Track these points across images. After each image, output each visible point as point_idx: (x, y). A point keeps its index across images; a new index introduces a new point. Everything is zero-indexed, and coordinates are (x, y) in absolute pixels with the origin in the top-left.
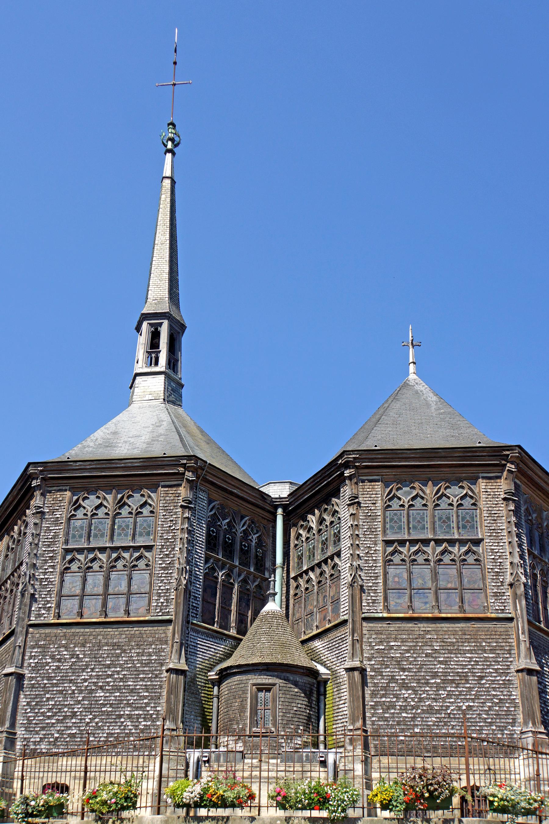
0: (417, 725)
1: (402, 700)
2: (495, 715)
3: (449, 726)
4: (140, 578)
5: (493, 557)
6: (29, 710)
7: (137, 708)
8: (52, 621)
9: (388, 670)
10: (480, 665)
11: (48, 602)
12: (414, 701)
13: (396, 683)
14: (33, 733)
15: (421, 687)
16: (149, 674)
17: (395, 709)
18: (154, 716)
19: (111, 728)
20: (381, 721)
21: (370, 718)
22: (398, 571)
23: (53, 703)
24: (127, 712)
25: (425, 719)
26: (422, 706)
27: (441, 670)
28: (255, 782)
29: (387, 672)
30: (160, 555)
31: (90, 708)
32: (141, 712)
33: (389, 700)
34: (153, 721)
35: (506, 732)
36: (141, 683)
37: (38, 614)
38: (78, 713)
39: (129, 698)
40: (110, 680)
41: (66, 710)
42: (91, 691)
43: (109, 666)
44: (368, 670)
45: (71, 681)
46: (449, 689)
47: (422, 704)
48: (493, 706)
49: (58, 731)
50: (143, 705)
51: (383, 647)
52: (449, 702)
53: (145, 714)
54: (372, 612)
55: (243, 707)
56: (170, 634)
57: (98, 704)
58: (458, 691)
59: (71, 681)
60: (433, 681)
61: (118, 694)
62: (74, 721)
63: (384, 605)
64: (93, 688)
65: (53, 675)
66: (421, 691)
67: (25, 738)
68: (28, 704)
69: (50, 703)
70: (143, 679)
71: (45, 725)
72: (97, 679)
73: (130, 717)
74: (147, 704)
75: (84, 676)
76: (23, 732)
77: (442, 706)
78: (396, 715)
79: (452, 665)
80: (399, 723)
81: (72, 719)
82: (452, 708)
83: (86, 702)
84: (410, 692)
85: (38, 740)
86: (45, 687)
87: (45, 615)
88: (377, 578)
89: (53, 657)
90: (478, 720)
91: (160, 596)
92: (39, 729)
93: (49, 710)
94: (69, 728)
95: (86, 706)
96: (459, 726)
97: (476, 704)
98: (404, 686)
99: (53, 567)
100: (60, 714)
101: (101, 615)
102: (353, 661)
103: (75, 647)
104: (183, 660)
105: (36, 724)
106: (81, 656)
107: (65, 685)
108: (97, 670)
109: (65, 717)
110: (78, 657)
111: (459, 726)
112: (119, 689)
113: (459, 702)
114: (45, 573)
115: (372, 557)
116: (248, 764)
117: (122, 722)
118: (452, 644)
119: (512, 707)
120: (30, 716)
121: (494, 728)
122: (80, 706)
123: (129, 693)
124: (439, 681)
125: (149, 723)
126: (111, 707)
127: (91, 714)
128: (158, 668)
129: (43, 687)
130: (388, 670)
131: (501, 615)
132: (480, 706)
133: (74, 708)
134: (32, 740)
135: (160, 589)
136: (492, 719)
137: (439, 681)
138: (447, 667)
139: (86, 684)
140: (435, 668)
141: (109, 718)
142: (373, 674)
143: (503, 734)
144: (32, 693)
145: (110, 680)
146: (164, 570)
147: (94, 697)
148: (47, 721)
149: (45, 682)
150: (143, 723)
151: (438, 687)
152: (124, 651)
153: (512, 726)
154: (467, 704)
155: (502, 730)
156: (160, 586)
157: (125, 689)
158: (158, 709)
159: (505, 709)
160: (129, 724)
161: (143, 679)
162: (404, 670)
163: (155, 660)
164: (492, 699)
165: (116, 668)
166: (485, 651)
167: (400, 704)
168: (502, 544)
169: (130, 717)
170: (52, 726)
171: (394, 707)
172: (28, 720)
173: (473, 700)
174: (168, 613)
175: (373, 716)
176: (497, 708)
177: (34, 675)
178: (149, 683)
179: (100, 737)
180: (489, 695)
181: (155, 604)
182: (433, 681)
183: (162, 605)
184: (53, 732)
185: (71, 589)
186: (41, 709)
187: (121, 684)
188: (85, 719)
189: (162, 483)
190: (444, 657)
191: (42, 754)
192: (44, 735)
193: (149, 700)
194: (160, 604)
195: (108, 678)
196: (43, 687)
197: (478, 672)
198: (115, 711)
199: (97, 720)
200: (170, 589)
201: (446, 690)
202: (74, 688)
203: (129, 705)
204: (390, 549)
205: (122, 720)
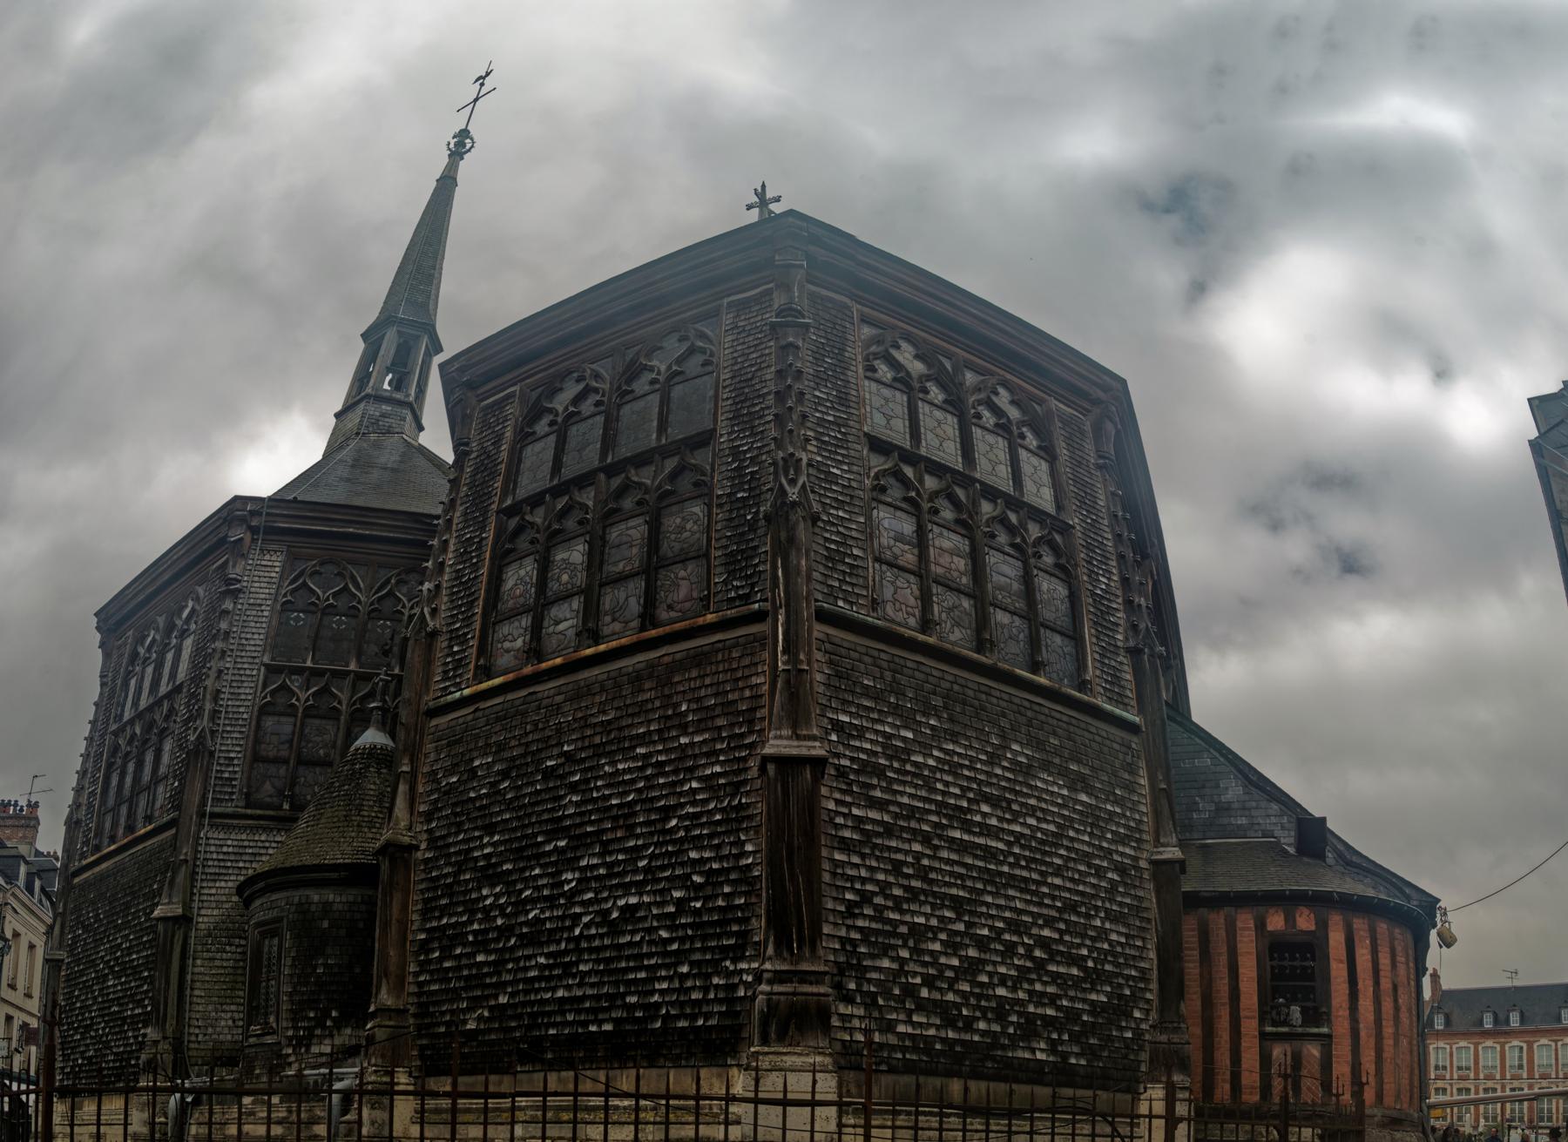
2: (690, 925)
46: (584, 863)
52: (583, 903)
58: (605, 864)
79: (598, 789)
82: (586, 919)
111: (597, 972)
113: (606, 900)
119: (740, 894)
121: (685, 969)
124: (562, 843)
137: (562, 843)
138: (588, 796)
143: (706, 989)
151: (567, 860)
153: (735, 961)
154: (621, 903)
155: (708, 976)
159: (720, 903)
164: (688, 876)
166: (684, 729)
173: (639, 887)
176: (698, 905)
180: (682, 864)
190: (581, 771)
197: (659, 798)
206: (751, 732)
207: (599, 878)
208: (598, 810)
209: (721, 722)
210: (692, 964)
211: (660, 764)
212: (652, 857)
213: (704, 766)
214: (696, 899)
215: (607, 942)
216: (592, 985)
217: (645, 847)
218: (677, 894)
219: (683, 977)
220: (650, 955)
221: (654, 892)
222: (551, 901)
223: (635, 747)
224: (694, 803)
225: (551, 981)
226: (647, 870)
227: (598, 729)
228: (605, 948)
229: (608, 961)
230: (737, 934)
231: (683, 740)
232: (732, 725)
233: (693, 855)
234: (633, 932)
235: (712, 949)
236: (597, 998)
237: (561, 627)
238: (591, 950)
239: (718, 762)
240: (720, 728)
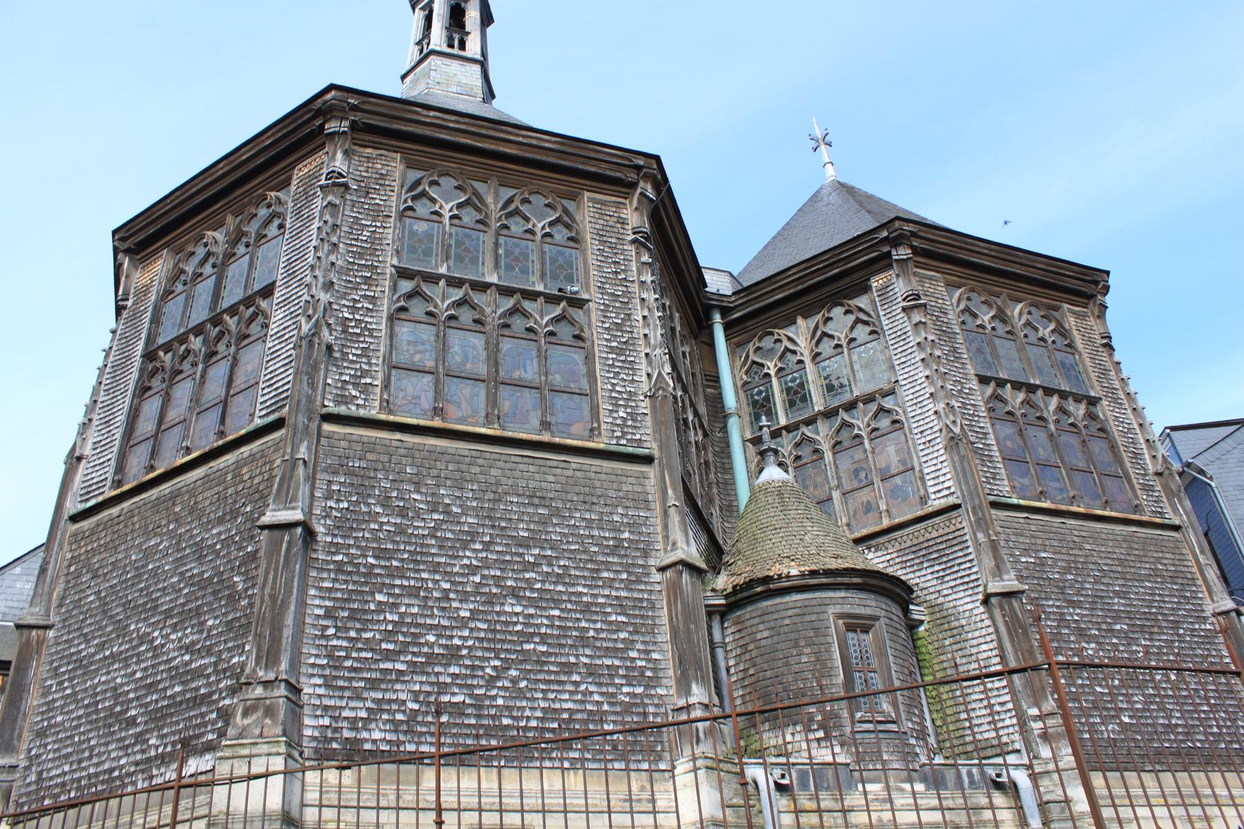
6: (331, 631)
11: (365, 373)
14: (347, 694)
18: (649, 674)
19: (552, 696)
23: (396, 618)
31: (493, 640)
32: (617, 663)
34: (647, 687)
36: (607, 592)
38: (464, 652)
41: (432, 638)
42: (490, 600)
43: (524, 543)
45: (435, 568)
50: (621, 646)
53: (627, 668)
55: (824, 666)
59: (435, 568)
61: (557, 613)
62: (454, 669)
64: (494, 590)
67: (326, 708)
68: (329, 614)
69: (389, 617)
70: (609, 583)
71: (378, 675)
73: (592, 671)
75: (470, 557)
76: (321, 691)
81: (449, 665)
85: (364, 714)
86: (369, 574)
87: (360, 402)
89: (385, 502)
92: (362, 684)
93: (389, 635)
95: (482, 635)
99: (372, 299)
100: (416, 650)
106: (455, 509)
112: (557, 602)
117: (576, 684)
122: (466, 633)
123: (581, 612)
125: (639, 690)
126: (543, 643)
128: (640, 562)
129: (365, 575)
133: (452, 637)
134: (346, 713)
139: (477, 579)
141: (541, 671)
144: (337, 586)
145: (533, 575)
147: (498, 613)
148: (382, 666)
149: (371, 560)
150: (625, 689)
152: (557, 512)
156: (613, 385)
157: (570, 601)
158: (655, 656)
160: (592, 688)
161: (609, 583)
163: (630, 541)
169: (592, 671)
170: (397, 681)
172: (330, 656)
178: (623, 594)
179: (528, 718)
184: (403, 696)
185: (412, 356)
186: (365, 630)
187: (560, 588)
188: (482, 668)
191: (376, 757)
195: (527, 571)
196: (365, 575)
199: (513, 673)
202: (447, 586)
203: (583, 641)
205: (576, 678)
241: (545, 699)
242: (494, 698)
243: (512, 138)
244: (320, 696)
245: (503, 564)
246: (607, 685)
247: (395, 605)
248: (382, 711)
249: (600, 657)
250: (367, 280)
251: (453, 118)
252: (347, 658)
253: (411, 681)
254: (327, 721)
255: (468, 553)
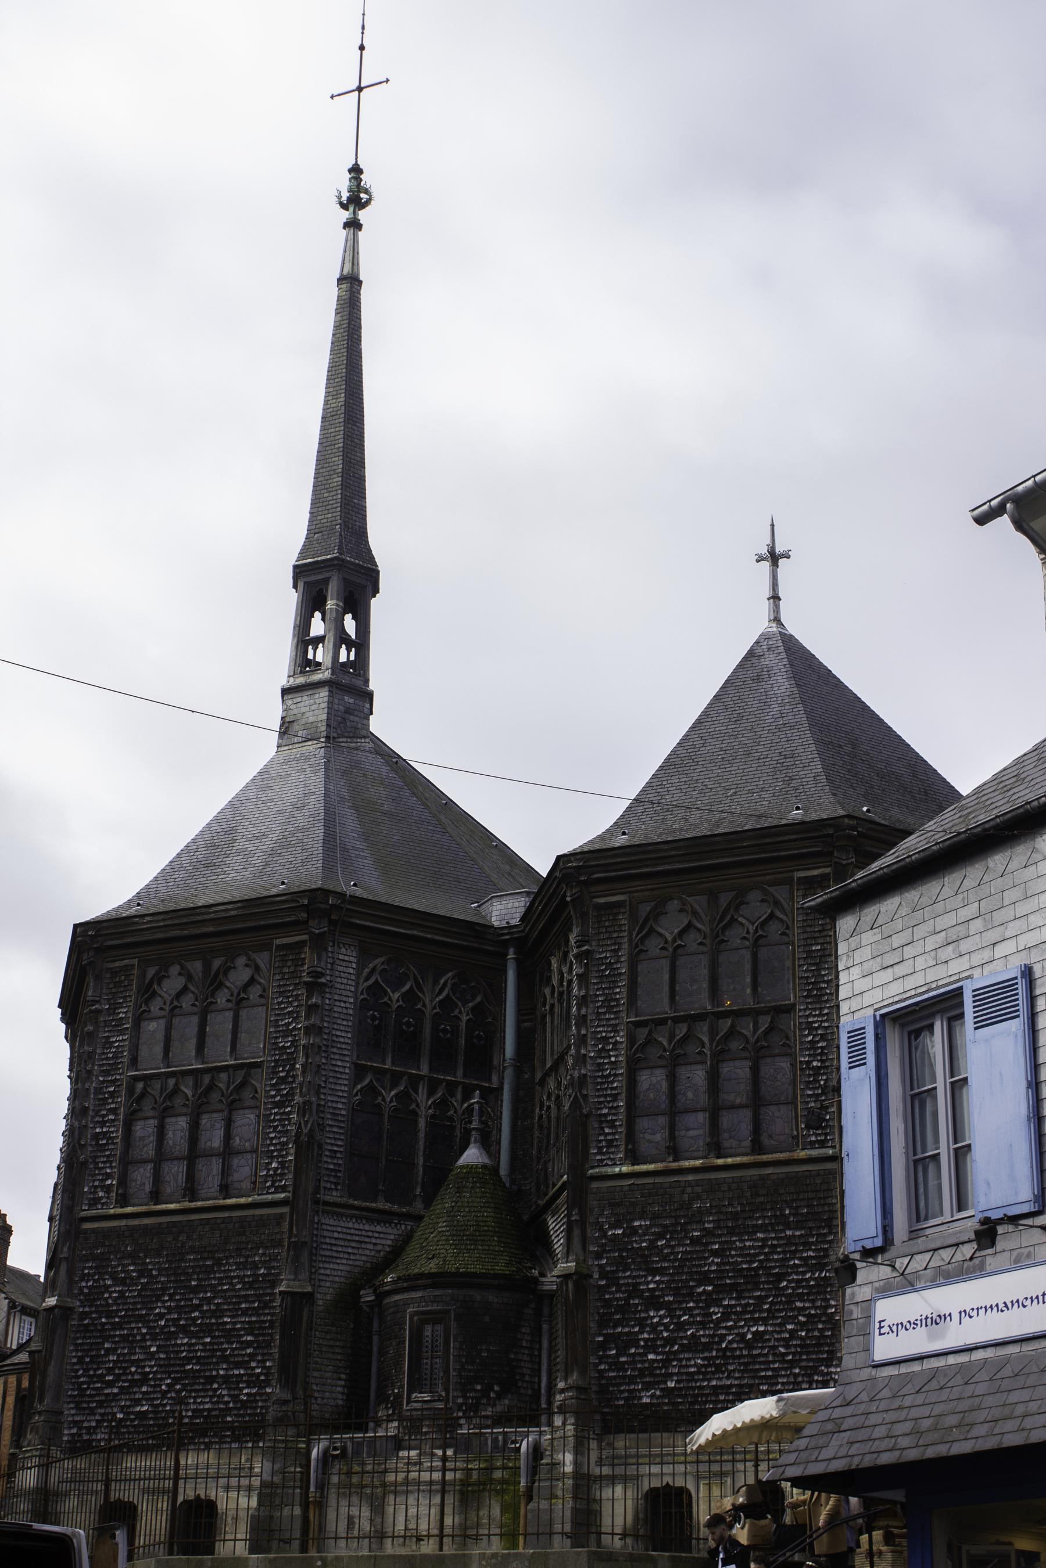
0: (672, 1374)
1: (648, 1329)
2: (800, 1346)
3: (723, 1373)
4: (246, 1121)
5: (810, 1038)
6: (81, 1372)
7: (238, 1365)
8: (112, 1211)
9: (628, 1273)
10: (779, 1253)
11: (109, 1176)
12: (667, 1329)
13: (641, 1297)
14: (87, 1412)
15: (680, 1303)
16: (254, 1302)
17: (637, 1347)
18: (262, 1378)
19: (199, 1400)
20: (613, 1371)
21: (596, 1365)
22: (654, 1080)
24: (221, 1372)
25: (684, 1363)
26: (682, 1338)
27: (714, 1268)
28: (412, 1492)
29: (625, 1276)
30: (272, 1079)
32: (242, 1372)
33: (626, 1330)
34: (260, 1388)
35: (816, 1378)
37: (94, 1199)
39: (225, 1346)
40: (197, 1314)
41: (133, 1369)
44: (596, 1276)
47: (681, 1334)
48: (797, 1331)
49: (122, 1407)
50: (246, 1359)
51: (620, 1232)
52: (726, 1328)
54: (607, 1165)
56: (286, 1224)
57: (180, 1359)
59: (140, 1318)
60: (701, 1289)
61: (208, 1340)
62: (144, 1389)
63: (626, 1151)
64: (172, 1329)
65: (115, 1308)
66: (681, 1309)
67: (75, 1422)
69: (111, 1358)
70: (245, 1312)
71: (103, 1398)
72: (179, 1313)
73: (226, 1380)
74: (252, 1357)
76: (73, 1412)
77: (713, 1336)
78: (638, 1358)
79: (733, 1256)
80: (642, 1373)
81: (141, 1386)
83: (162, 1356)
84: (662, 1312)
85: (94, 1424)
88: (615, 1098)
89: (114, 1276)
90: (771, 1358)
91: (272, 1158)
93: (110, 1371)
94: (138, 1402)
96: (739, 1371)
97: (770, 1328)
98: (654, 1302)
99: (114, 1111)
100: (124, 1378)
101: (184, 1196)
102: (567, 1262)
103: (146, 1257)
104: (304, 1275)
105: (90, 1396)
106: (154, 1273)
107: (133, 1325)
108: (178, 1297)
109: (133, 1383)
110: (151, 1276)
113: (742, 1327)
114: (103, 1124)
115: (610, 1057)
116: (403, 1458)
117: (216, 1390)
118: (735, 1216)
119: (828, 1329)
120: (83, 1383)
121: (797, 1371)
124: (710, 1288)
125: (254, 1391)
127: (169, 1377)
128: (269, 1291)
130: (628, 1273)
131: (815, 1153)
132: (775, 1331)
133: (144, 1367)
135: (271, 1144)
136: (794, 1354)
140: (705, 1265)
141: (194, 1384)
142: (603, 1283)
145: (197, 1314)
146: (280, 1108)
151: (711, 1300)
154: (755, 1329)
155: (811, 1375)
156: (272, 1139)
157: (218, 1330)
159: (816, 1333)
160: (225, 1392)
161: (245, 1312)
162: (654, 1272)
164: (796, 1317)
165: (206, 1292)
167: (646, 1336)
168: (826, 1011)
171: (635, 1343)
172: (80, 1389)
173: (764, 1321)
174: (283, 1189)
175: (601, 1363)
177: (87, 1309)
178: (254, 1319)
180: (792, 1310)
181: (265, 1173)
182: (701, 1289)
183: (275, 1174)
184: (115, 1410)
186: (98, 1369)
187: (213, 1321)
188: (161, 1386)
189: (278, 942)
190: (720, 1243)
192: (101, 1415)
193: (255, 1348)
194: (271, 1172)
195: (194, 1312)
197: (774, 1267)
198: (205, 1371)
200: (286, 1143)
201: (722, 1306)
202: (144, 1331)
203: (224, 1359)
204: (642, 1034)
205: (215, 1386)
206: (830, 1233)
207: (735, 1313)
208: (733, 1270)
209: (810, 1224)
210: (801, 1368)
211: (775, 1246)
212: (772, 1303)
213: (802, 1251)
214: (802, 1331)
215: (745, 1352)
216: (736, 1378)
217: (767, 1297)
218: (790, 1327)
219: (796, 1376)
220: (774, 1362)
221: (775, 1325)
222: (703, 1325)
223: (756, 1232)
224: (797, 1273)
225: (707, 1376)
226: (768, 1311)
227: (729, 1216)
228: (744, 1356)
229: (748, 1363)
230: (828, 1352)
231: (789, 1233)
232: (819, 1228)
233: (799, 1304)
234: (762, 1348)
235: (813, 1360)
236: (740, 1386)
237: (691, 1133)
238: (734, 1357)
239: (811, 1249)
240: (811, 1228)
241: (195, 1403)
242: (165, 1405)
243: (206, 917)
244: (73, 1415)
245: (179, 1309)
246: (234, 1389)
247: (116, 1349)
248: (104, 1421)
249: (232, 1369)
250: (112, 1094)
251: (161, 917)
252: (88, 1388)
253: (121, 1399)
254: (74, 1431)
255: (159, 1304)
